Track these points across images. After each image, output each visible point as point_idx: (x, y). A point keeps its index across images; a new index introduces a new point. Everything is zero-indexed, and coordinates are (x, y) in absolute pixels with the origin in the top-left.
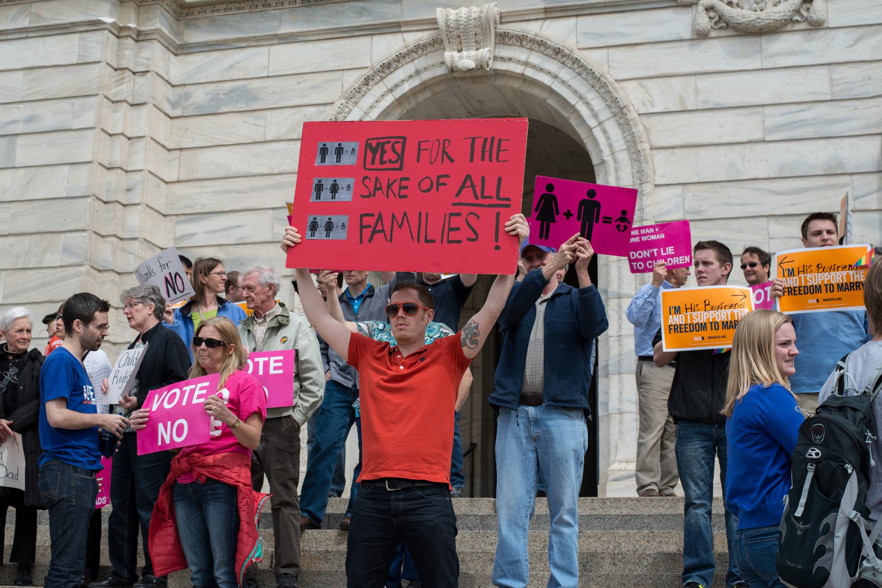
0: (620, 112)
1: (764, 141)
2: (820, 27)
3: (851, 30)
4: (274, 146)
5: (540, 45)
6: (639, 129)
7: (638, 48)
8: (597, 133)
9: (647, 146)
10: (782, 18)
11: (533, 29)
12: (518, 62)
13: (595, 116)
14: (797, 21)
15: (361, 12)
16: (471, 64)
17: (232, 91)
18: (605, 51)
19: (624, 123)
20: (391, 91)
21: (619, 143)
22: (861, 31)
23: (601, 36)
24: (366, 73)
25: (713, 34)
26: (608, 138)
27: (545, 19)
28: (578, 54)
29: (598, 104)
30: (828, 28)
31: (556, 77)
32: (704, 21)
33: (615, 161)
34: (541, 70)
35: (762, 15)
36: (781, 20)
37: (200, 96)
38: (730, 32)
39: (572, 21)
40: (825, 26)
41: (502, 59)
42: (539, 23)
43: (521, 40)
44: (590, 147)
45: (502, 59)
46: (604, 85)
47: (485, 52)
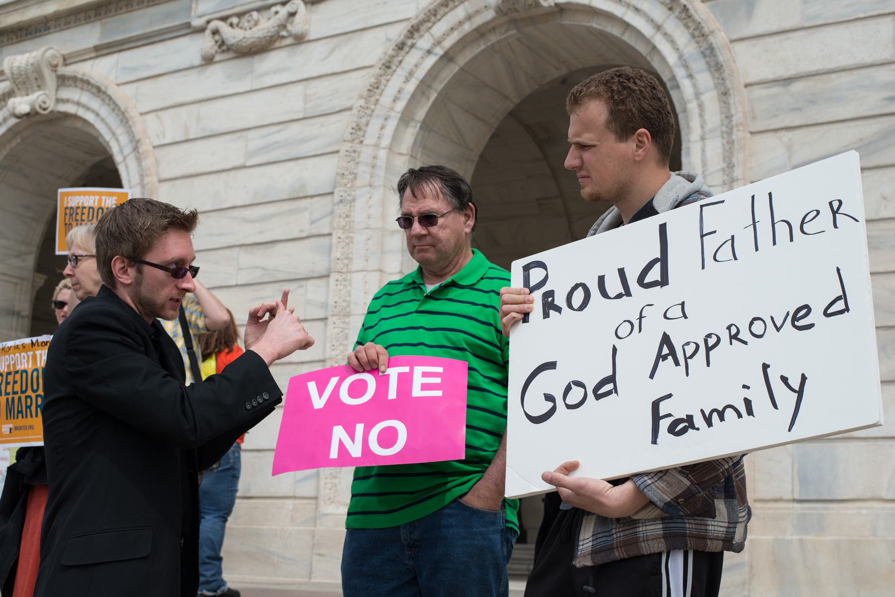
1: (244, 167)
2: (301, 41)
3: (327, 40)
7: (160, 79)
10: (265, 35)
14: (283, 37)
18: (134, 85)
22: (336, 40)
23: (134, 69)
27: (97, 57)
30: (309, 41)
36: (265, 37)
38: (231, 55)
40: (307, 39)
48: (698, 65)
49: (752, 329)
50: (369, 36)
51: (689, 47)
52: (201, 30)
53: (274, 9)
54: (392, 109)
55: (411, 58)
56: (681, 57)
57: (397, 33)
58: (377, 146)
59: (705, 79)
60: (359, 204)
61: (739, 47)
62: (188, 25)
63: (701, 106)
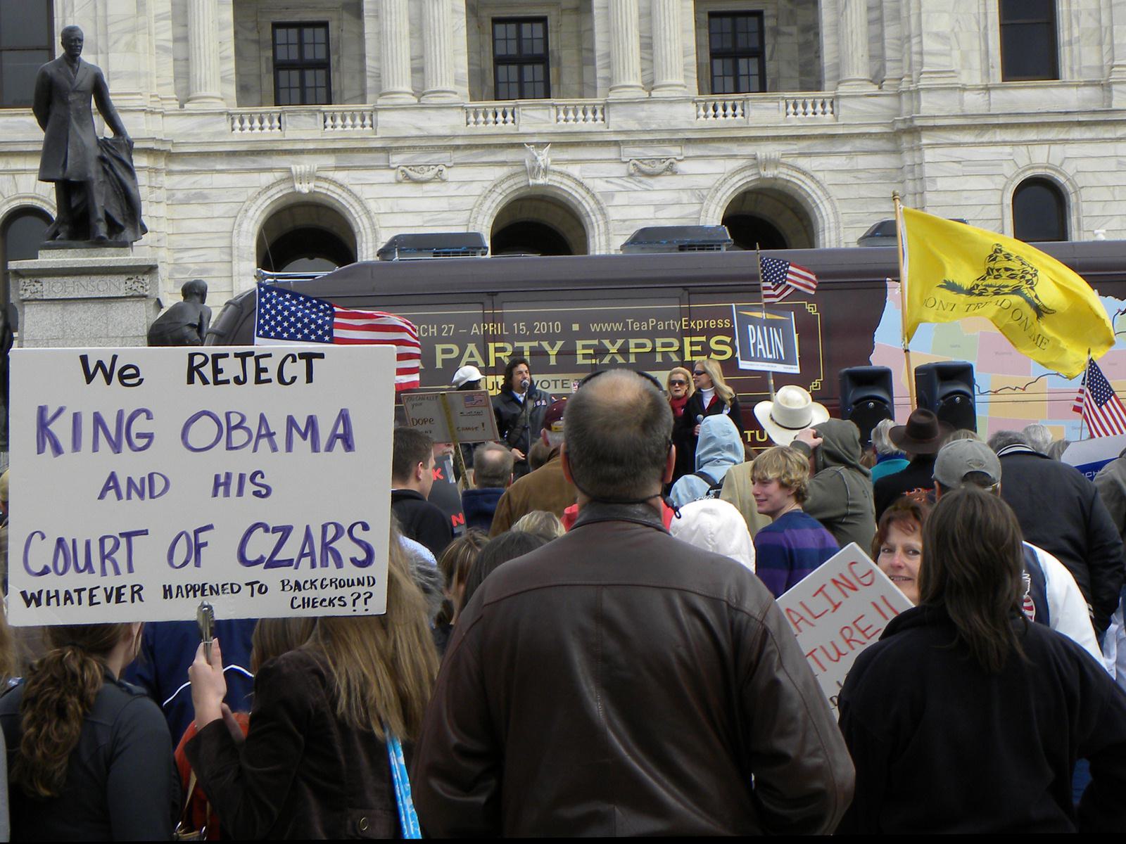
0: (368, 212)
4: (218, 220)
5: (334, 182)
6: (375, 220)
8: (358, 220)
11: (331, 175)
13: (357, 213)
15: (254, 162)
16: (306, 191)
17: (196, 194)
19: (370, 218)
20: (269, 198)
21: (367, 225)
23: (359, 179)
24: (259, 190)
28: (350, 187)
29: (358, 208)
31: (340, 196)
32: (400, 177)
35: (424, 176)
37: (179, 195)
39: (347, 172)
41: (318, 187)
43: (326, 179)
44: (354, 225)
45: (318, 187)
46: (361, 201)
47: (312, 185)
48: (597, 212)
49: (164, 481)
51: (594, 206)
55: (494, 195)
57: (489, 185)
59: (599, 217)
61: (610, 208)
63: (598, 225)
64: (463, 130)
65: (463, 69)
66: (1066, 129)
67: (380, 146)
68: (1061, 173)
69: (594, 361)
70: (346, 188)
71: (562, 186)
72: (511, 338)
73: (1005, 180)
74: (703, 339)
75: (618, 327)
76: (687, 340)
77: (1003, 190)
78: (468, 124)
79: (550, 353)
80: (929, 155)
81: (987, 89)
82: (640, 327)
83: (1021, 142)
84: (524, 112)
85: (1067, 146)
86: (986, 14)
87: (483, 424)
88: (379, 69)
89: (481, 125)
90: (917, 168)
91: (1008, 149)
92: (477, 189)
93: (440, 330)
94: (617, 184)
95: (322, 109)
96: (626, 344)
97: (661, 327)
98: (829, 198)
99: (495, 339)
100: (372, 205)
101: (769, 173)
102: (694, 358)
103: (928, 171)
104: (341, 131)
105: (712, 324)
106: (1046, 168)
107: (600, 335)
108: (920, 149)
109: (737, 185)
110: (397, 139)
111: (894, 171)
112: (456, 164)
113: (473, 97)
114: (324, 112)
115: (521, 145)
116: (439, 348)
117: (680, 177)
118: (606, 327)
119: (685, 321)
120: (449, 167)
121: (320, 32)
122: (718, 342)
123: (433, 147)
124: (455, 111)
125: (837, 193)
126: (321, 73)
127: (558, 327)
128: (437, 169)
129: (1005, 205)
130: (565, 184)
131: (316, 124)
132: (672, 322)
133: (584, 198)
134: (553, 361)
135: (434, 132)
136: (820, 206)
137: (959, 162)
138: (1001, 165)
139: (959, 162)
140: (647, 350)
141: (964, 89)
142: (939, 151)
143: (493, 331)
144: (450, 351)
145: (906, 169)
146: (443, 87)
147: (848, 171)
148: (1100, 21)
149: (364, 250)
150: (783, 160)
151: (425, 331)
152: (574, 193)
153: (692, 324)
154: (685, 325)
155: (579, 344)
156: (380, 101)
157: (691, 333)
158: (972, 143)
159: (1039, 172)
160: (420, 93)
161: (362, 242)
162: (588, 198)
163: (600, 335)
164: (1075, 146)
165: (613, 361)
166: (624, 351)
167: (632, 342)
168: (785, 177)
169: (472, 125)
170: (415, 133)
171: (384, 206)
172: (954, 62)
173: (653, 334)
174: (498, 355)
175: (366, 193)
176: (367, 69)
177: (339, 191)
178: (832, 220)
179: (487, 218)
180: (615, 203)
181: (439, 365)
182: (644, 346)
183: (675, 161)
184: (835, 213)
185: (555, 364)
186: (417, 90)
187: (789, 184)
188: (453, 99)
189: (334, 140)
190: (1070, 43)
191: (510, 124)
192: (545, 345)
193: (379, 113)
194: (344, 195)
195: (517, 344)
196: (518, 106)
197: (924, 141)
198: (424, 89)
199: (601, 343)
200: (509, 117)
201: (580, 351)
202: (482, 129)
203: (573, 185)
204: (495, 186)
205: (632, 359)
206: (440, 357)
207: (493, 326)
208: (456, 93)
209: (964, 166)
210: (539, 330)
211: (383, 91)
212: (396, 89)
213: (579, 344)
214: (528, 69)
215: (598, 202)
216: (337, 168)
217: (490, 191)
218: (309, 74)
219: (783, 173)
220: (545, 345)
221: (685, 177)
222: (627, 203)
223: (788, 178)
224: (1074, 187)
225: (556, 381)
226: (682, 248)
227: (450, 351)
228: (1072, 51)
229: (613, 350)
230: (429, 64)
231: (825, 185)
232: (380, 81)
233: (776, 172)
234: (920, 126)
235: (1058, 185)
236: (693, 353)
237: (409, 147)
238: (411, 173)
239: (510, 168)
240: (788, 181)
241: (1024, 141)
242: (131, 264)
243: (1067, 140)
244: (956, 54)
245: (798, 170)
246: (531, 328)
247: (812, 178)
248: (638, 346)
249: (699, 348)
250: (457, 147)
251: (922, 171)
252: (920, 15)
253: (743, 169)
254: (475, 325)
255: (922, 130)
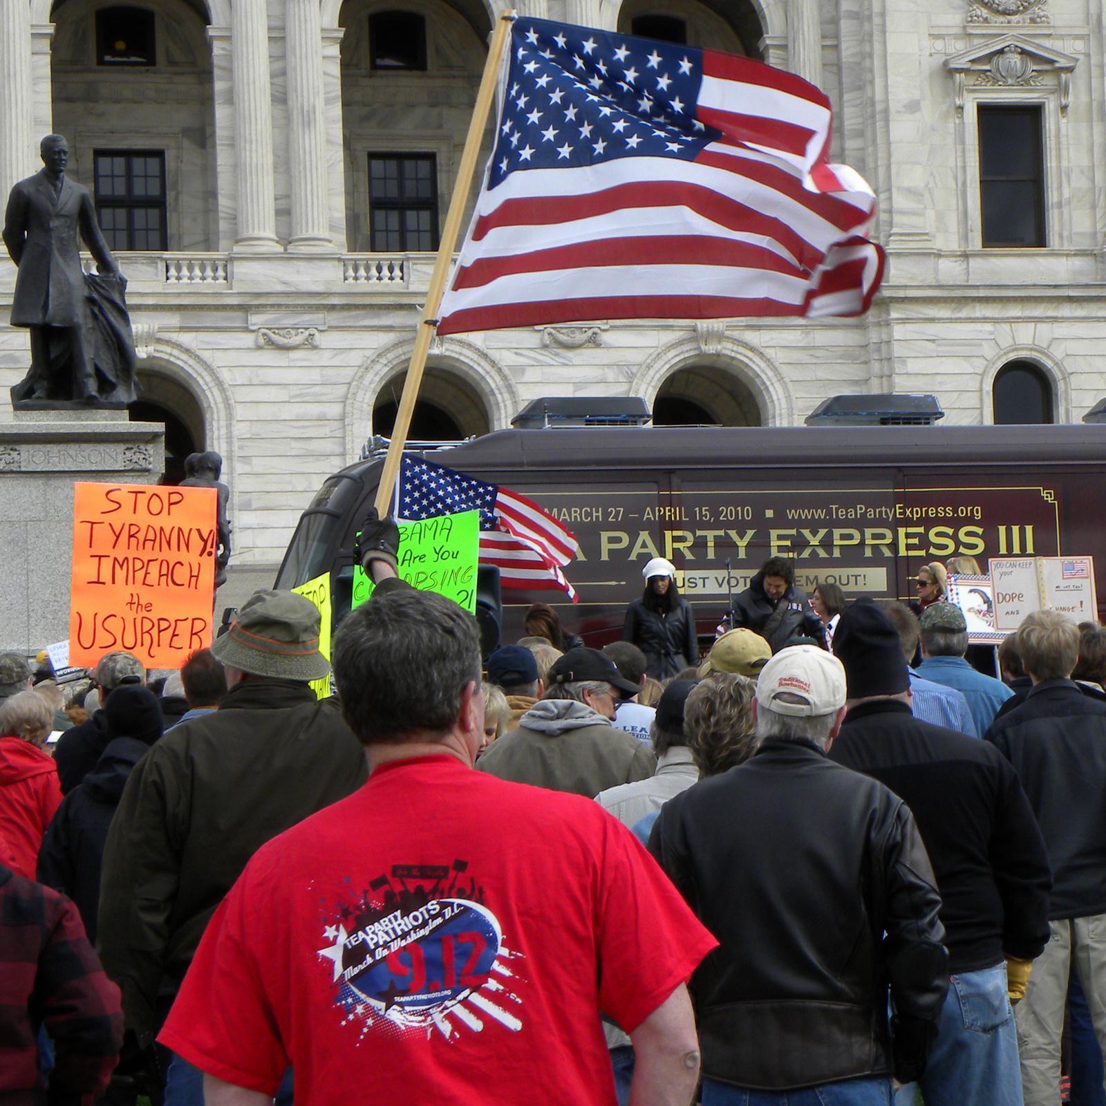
0: (220, 384)
1: (289, 402)
5: (178, 346)
6: (229, 393)
8: (208, 392)
9: (233, 401)
11: (174, 337)
12: (166, 353)
19: (223, 390)
21: (219, 400)
22: (335, 352)
23: (209, 343)
25: (266, 347)
26: (213, 396)
28: (198, 352)
29: (208, 379)
31: (186, 363)
32: (262, 341)
33: (217, 407)
34: (179, 358)
35: (290, 341)
39: (195, 333)
41: (158, 351)
42: (177, 334)
46: (212, 370)
47: (151, 349)
48: (504, 390)
50: (354, 352)
51: (501, 383)
52: (254, 331)
53: (300, 330)
54: (369, 387)
55: (378, 367)
56: (497, 385)
58: (362, 402)
59: (506, 396)
60: (355, 426)
61: (519, 386)
62: (247, 328)
63: (505, 406)
64: (340, 287)
65: (340, 213)
66: (1055, 304)
67: (237, 303)
68: (1048, 357)
69: (791, 555)
70: (193, 353)
71: (462, 358)
72: (693, 526)
73: (985, 363)
74: (921, 530)
75: (820, 514)
76: (902, 531)
77: (983, 375)
78: (346, 279)
79: (739, 544)
80: (899, 331)
81: (966, 256)
82: (847, 515)
83: (1003, 318)
84: (415, 267)
85: (1055, 325)
86: (964, 168)
87: (1081, 602)
88: (235, 210)
89: (363, 280)
90: (884, 346)
91: (988, 327)
92: (356, 358)
93: (606, 514)
94: (528, 357)
95: (164, 256)
96: (829, 536)
97: (871, 514)
98: (781, 379)
99: (673, 526)
100: (226, 375)
101: (711, 348)
102: (912, 553)
103: (898, 350)
104: (188, 284)
105: (932, 512)
106: (1031, 349)
107: (800, 524)
108: (888, 324)
109: (673, 362)
110: (258, 295)
111: (857, 349)
112: (331, 328)
113: (353, 247)
114: (166, 260)
115: (412, 307)
116: (605, 536)
117: (605, 350)
118: (806, 514)
119: (900, 508)
120: (322, 331)
121: (153, 163)
122: (938, 534)
123: (302, 306)
124: (330, 264)
125: (789, 373)
126: (154, 213)
127: (748, 513)
128: (307, 333)
129: (984, 391)
130: (465, 356)
131: (157, 275)
132: (884, 509)
133: (488, 373)
134: (742, 554)
135: (304, 288)
136: (771, 388)
137: (933, 341)
138: (981, 345)
139: (933, 341)
140: (855, 542)
141: (939, 255)
142: (909, 327)
143: (670, 516)
144: (619, 540)
145: (872, 347)
146: (316, 234)
147: (804, 348)
148: (1093, 181)
149: (215, 429)
150: (727, 333)
151: (588, 514)
152: (476, 366)
153: (908, 512)
154: (900, 514)
155: (774, 533)
156: (236, 249)
157: (908, 522)
158: (947, 319)
159: (1023, 354)
160: (286, 239)
161: (213, 419)
162: (493, 373)
163: (800, 524)
164: (1063, 325)
165: (814, 554)
166: (827, 544)
167: (837, 533)
168: (728, 353)
169: (351, 281)
170: (280, 288)
171: (240, 377)
172: (927, 222)
173: (861, 524)
174: (676, 545)
175: (217, 360)
176: (220, 208)
177: (184, 357)
178: (784, 405)
179: (369, 394)
180: (525, 379)
181: (605, 557)
182: (850, 537)
183: (599, 331)
184: (788, 397)
185: (744, 557)
186: (282, 236)
187: (734, 362)
188: (328, 248)
189: (179, 295)
190: (1060, 205)
191: (398, 280)
192: (733, 534)
193: (236, 263)
194: (191, 362)
195: (699, 533)
196: (408, 259)
197: (894, 315)
198: (290, 235)
199: (800, 534)
200: (397, 272)
201: (775, 543)
202: (363, 285)
203: (475, 357)
204: (379, 355)
205: (837, 553)
206: (605, 547)
207: (670, 511)
208: (330, 241)
209: (938, 345)
210: (726, 516)
211: (239, 237)
212: (256, 234)
213: (774, 533)
214: (411, 216)
215: (505, 378)
216: (182, 329)
217: (373, 361)
218: (139, 214)
219: (727, 348)
220: (733, 534)
221: (611, 350)
222: (540, 380)
223: (733, 354)
224: (1062, 373)
225: (745, 578)
226: (884, 422)
227: (619, 540)
228: (1061, 214)
229: (814, 541)
230: (298, 206)
231: (777, 364)
232: (236, 224)
233: (719, 347)
234: (889, 297)
235: (1044, 370)
236: (909, 547)
237: (272, 306)
238: (275, 338)
239: (398, 334)
240: (733, 358)
241: (1008, 318)
242: (132, 430)
243: (1056, 318)
244: (931, 214)
245: (746, 345)
246: (715, 513)
247: (761, 355)
248: (843, 537)
249: (916, 541)
250: (332, 308)
251: (890, 351)
252: (889, 167)
253: (680, 343)
254: (648, 509)
255: (891, 302)
